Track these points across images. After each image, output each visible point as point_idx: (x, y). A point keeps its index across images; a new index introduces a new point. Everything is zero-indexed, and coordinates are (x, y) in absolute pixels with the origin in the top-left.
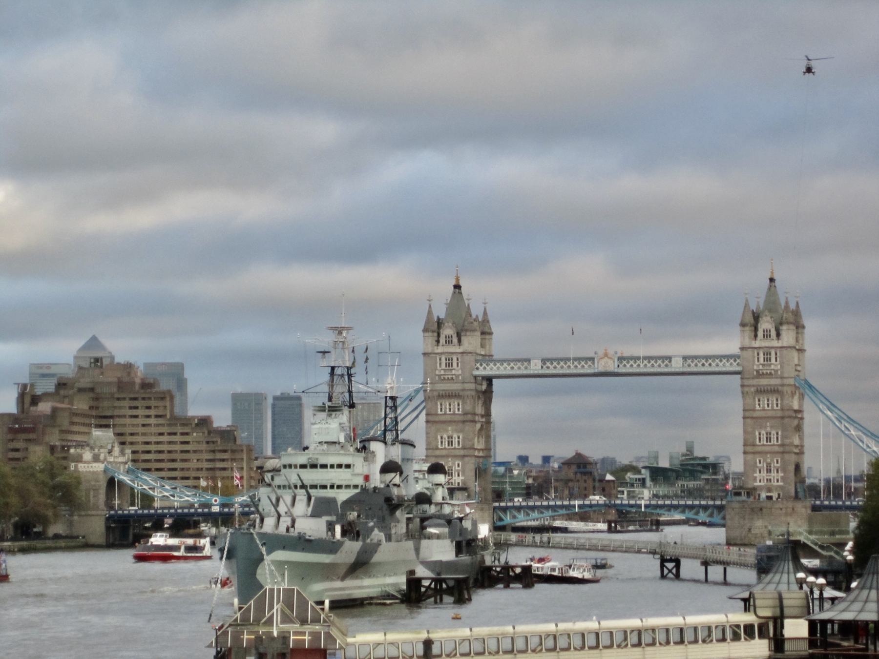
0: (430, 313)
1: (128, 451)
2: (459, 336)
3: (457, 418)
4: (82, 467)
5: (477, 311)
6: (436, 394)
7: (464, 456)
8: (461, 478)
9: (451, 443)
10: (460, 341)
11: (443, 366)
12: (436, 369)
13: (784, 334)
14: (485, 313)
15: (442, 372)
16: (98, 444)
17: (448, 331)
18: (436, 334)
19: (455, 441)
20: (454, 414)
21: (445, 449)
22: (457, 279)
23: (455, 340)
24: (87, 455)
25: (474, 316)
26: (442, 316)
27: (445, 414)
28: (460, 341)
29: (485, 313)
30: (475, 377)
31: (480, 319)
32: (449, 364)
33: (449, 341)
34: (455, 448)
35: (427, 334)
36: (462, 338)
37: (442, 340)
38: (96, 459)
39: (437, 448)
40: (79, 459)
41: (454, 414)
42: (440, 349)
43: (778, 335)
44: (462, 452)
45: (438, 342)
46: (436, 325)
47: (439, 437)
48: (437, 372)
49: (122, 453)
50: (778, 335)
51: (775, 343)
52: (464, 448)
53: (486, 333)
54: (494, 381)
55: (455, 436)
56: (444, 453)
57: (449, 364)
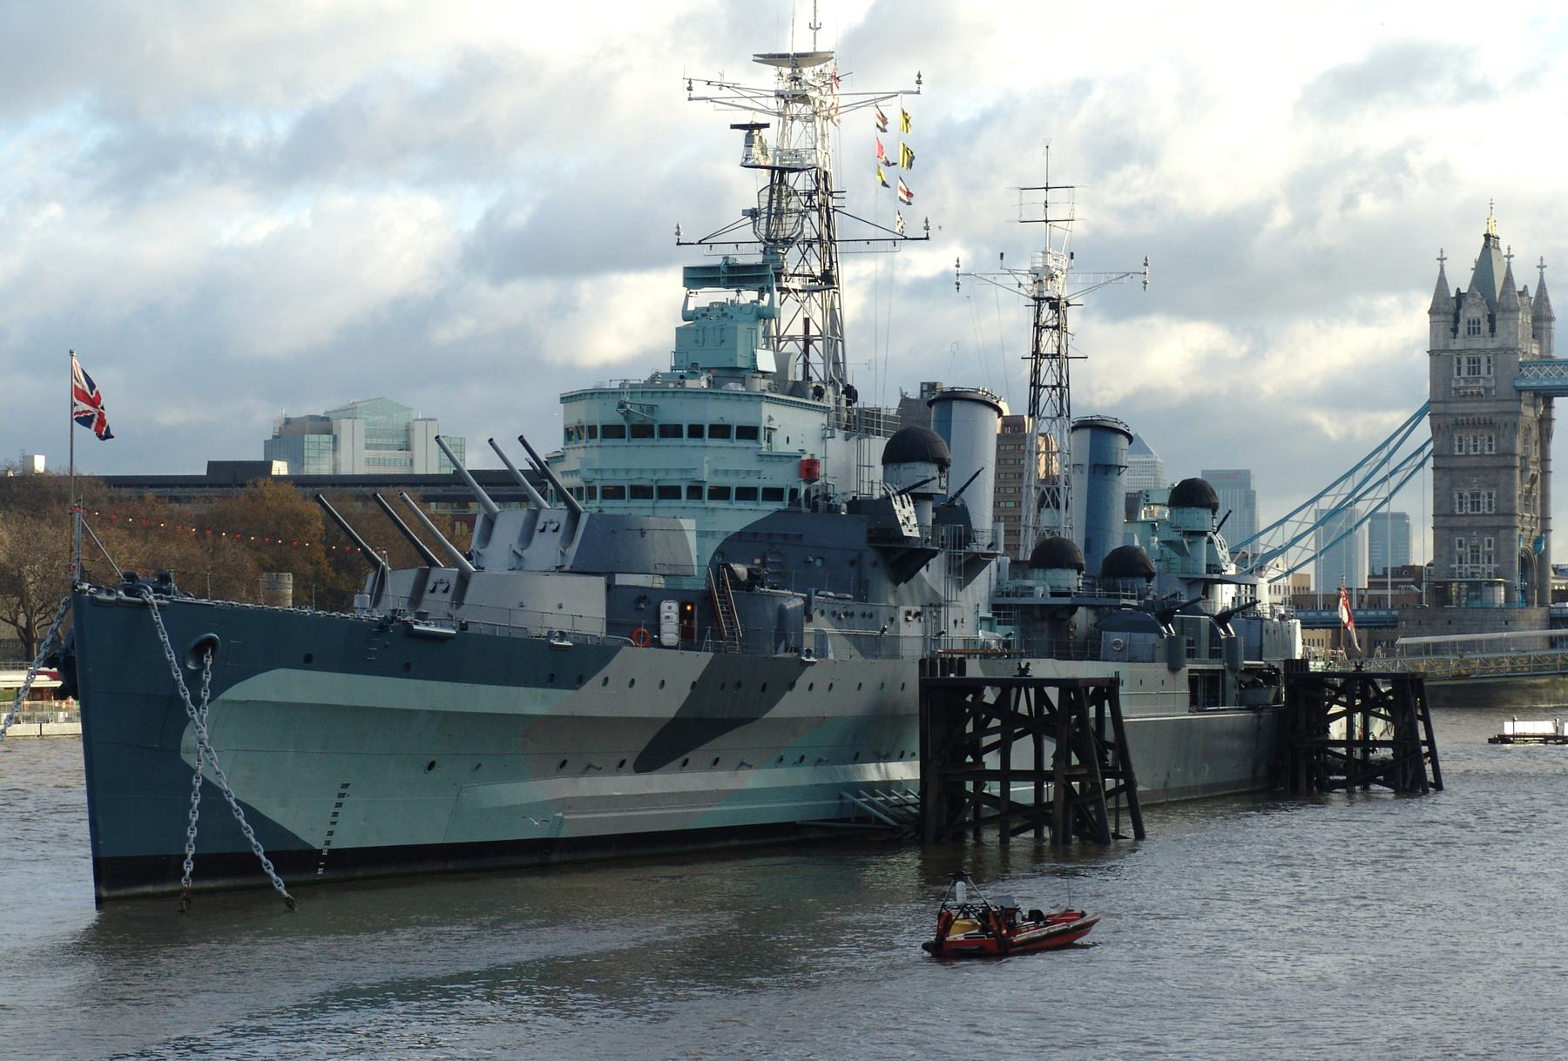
2: (1491, 319)
3: (1487, 463)
5: (1525, 278)
6: (1450, 420)
7: (1499, 527)
8: (1493, 565)
9: (1476, 505)
10: (1492, 329)
11: (1464, 374)
12: (1451, 378)
14: (1542, 286)
15: (1462, 383)
17: (1473, 312)
18: (1451, 318)
19: (1484, 501)
20: (1482, 455)
21: (1466, 515)
23: (1485, 327)
25: (1519, 288)
26: (1464, 290)
27: (1467, 455)
28: (1492, 329)
29: (1542, 286)
30: (1520, 390)
31: (1532, 293)
32: (1474, 369)
33: (1473, 329)
34: (1484, 514)
35: (1436, 318)
36: (1498, 323)
37: (1462, 328)
39: (1454, 515)
41: (1482, 455)
42: (1458, 344)
44: (1496, 521)
45: (1455, 330)
46: (1454, 303)
47: (1456, 496)
48: (1453, 384)
52: (1496, 514)
53: (1541, 316)
54: (1557, 401)
55: (1484, 492)
56: (1466, 522)
57: (1474, 369)
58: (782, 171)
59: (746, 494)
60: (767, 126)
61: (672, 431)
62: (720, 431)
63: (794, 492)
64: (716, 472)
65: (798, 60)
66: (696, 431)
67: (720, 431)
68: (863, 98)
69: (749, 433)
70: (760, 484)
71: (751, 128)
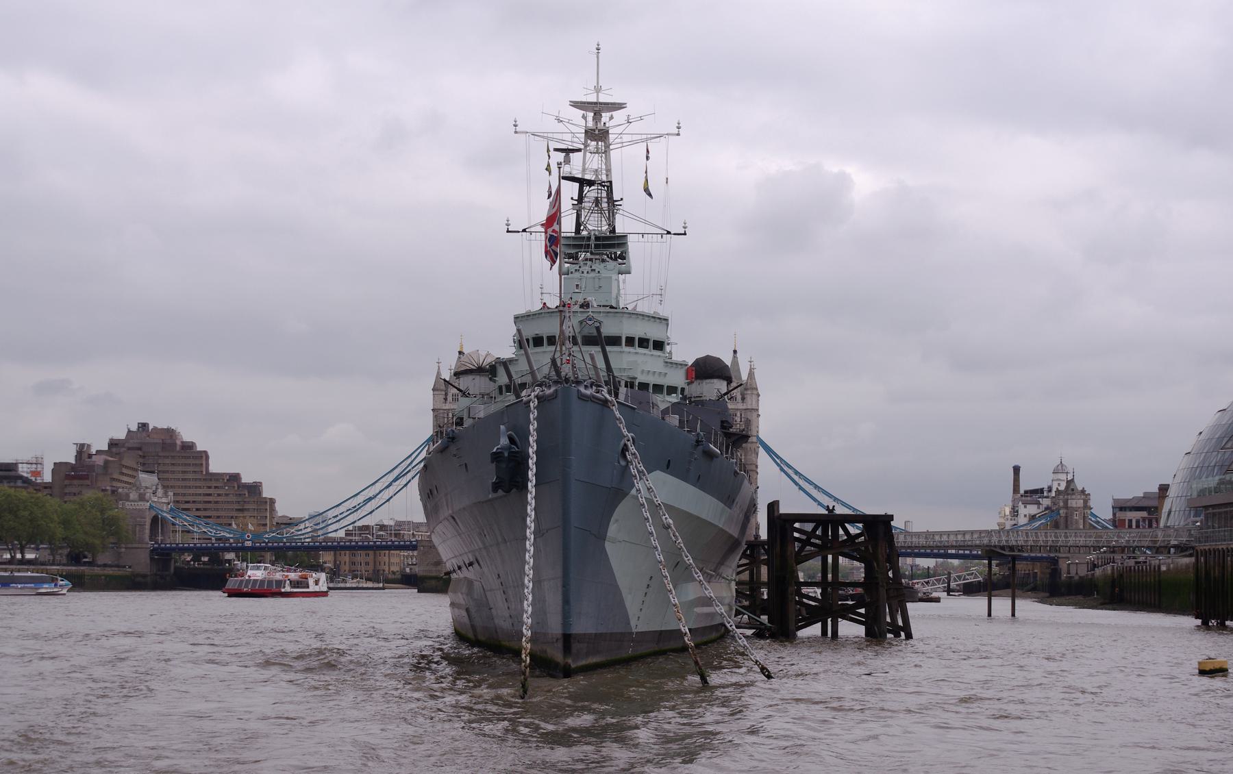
0: (439, 373)
1: (171, 494)
4: (128, 505)
13: (748, 398)
16: (143, 485)
22: (462, 347)
24: (133, 495)
37: (450, 398)
38: (142, 498)
40: (127, 498)
42: (447, 406)
43: (743, 399)
45: (446, 399)
49: (166, 495)
50: (743, 399)
51: (740, 406)
58: (583, 182)
59: (658, 388)
60: (579, 150)
61: (614, 341)
62: (643, 343)
63: (683, 390)
64: (643, 371)
65: (598, 108)
66: (630, 341)
67: (643, 343)
68: (639, 137)
69: (659, 345)
70: (666, 382)
71: (567, 151)
